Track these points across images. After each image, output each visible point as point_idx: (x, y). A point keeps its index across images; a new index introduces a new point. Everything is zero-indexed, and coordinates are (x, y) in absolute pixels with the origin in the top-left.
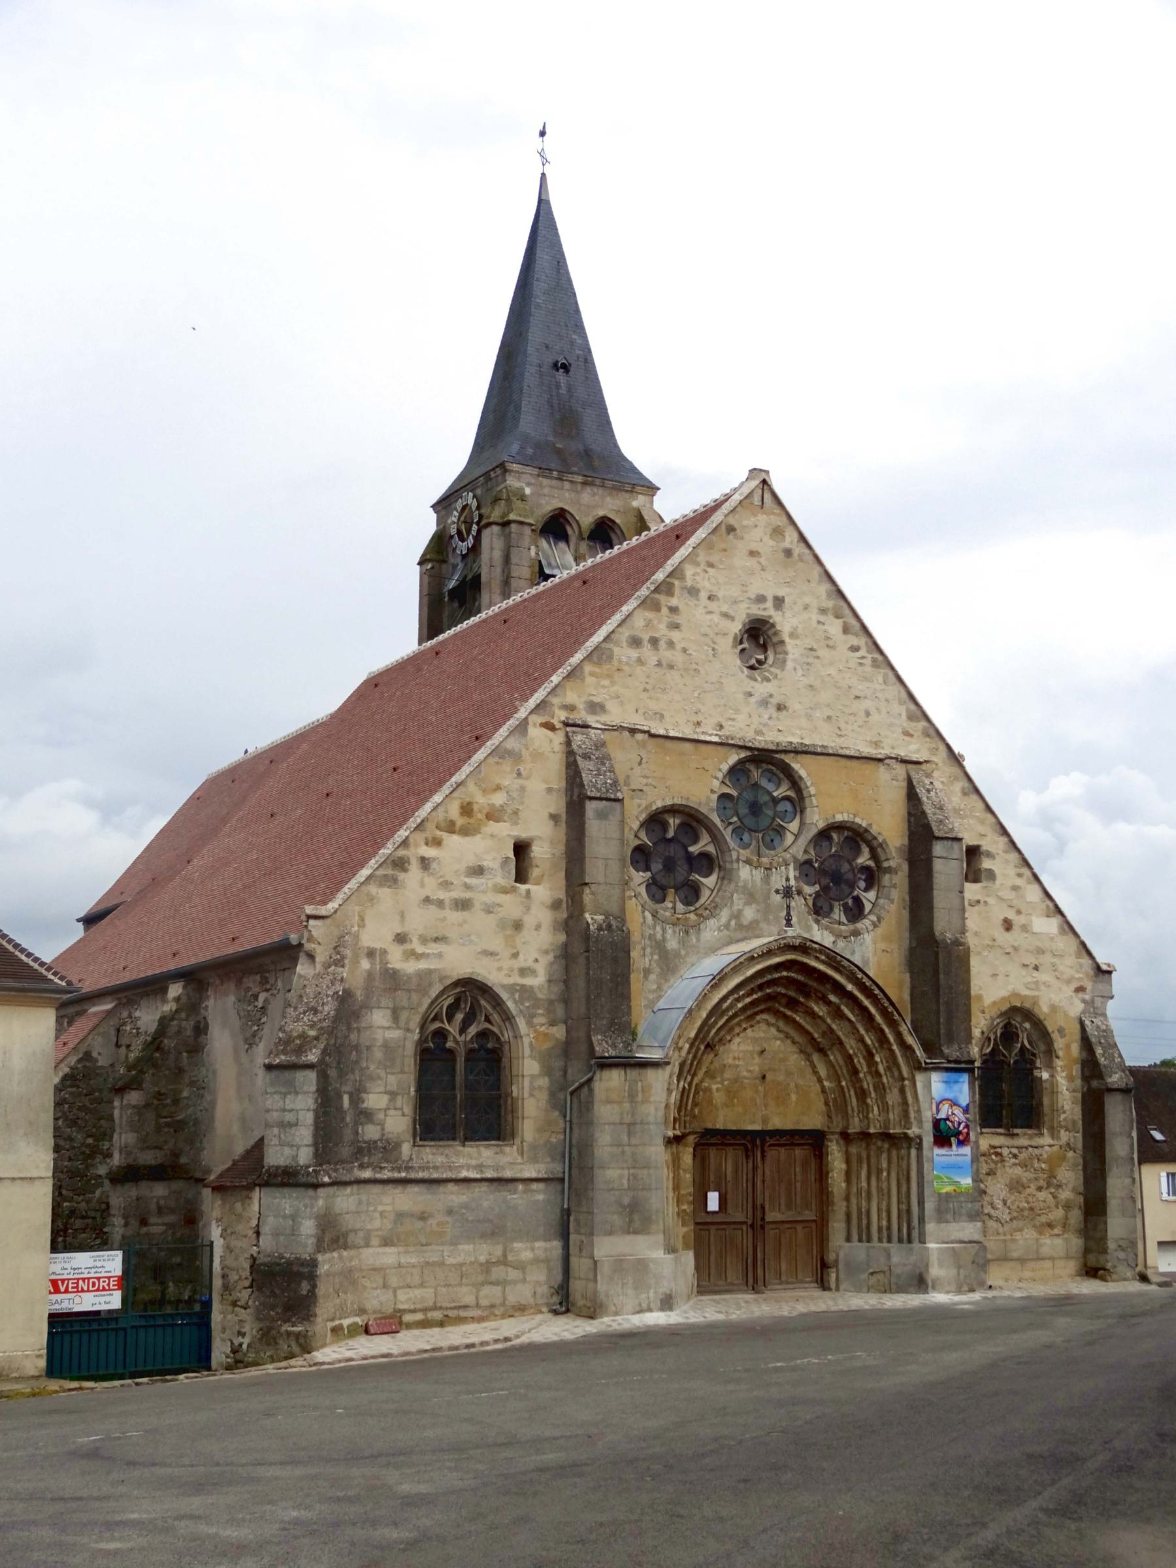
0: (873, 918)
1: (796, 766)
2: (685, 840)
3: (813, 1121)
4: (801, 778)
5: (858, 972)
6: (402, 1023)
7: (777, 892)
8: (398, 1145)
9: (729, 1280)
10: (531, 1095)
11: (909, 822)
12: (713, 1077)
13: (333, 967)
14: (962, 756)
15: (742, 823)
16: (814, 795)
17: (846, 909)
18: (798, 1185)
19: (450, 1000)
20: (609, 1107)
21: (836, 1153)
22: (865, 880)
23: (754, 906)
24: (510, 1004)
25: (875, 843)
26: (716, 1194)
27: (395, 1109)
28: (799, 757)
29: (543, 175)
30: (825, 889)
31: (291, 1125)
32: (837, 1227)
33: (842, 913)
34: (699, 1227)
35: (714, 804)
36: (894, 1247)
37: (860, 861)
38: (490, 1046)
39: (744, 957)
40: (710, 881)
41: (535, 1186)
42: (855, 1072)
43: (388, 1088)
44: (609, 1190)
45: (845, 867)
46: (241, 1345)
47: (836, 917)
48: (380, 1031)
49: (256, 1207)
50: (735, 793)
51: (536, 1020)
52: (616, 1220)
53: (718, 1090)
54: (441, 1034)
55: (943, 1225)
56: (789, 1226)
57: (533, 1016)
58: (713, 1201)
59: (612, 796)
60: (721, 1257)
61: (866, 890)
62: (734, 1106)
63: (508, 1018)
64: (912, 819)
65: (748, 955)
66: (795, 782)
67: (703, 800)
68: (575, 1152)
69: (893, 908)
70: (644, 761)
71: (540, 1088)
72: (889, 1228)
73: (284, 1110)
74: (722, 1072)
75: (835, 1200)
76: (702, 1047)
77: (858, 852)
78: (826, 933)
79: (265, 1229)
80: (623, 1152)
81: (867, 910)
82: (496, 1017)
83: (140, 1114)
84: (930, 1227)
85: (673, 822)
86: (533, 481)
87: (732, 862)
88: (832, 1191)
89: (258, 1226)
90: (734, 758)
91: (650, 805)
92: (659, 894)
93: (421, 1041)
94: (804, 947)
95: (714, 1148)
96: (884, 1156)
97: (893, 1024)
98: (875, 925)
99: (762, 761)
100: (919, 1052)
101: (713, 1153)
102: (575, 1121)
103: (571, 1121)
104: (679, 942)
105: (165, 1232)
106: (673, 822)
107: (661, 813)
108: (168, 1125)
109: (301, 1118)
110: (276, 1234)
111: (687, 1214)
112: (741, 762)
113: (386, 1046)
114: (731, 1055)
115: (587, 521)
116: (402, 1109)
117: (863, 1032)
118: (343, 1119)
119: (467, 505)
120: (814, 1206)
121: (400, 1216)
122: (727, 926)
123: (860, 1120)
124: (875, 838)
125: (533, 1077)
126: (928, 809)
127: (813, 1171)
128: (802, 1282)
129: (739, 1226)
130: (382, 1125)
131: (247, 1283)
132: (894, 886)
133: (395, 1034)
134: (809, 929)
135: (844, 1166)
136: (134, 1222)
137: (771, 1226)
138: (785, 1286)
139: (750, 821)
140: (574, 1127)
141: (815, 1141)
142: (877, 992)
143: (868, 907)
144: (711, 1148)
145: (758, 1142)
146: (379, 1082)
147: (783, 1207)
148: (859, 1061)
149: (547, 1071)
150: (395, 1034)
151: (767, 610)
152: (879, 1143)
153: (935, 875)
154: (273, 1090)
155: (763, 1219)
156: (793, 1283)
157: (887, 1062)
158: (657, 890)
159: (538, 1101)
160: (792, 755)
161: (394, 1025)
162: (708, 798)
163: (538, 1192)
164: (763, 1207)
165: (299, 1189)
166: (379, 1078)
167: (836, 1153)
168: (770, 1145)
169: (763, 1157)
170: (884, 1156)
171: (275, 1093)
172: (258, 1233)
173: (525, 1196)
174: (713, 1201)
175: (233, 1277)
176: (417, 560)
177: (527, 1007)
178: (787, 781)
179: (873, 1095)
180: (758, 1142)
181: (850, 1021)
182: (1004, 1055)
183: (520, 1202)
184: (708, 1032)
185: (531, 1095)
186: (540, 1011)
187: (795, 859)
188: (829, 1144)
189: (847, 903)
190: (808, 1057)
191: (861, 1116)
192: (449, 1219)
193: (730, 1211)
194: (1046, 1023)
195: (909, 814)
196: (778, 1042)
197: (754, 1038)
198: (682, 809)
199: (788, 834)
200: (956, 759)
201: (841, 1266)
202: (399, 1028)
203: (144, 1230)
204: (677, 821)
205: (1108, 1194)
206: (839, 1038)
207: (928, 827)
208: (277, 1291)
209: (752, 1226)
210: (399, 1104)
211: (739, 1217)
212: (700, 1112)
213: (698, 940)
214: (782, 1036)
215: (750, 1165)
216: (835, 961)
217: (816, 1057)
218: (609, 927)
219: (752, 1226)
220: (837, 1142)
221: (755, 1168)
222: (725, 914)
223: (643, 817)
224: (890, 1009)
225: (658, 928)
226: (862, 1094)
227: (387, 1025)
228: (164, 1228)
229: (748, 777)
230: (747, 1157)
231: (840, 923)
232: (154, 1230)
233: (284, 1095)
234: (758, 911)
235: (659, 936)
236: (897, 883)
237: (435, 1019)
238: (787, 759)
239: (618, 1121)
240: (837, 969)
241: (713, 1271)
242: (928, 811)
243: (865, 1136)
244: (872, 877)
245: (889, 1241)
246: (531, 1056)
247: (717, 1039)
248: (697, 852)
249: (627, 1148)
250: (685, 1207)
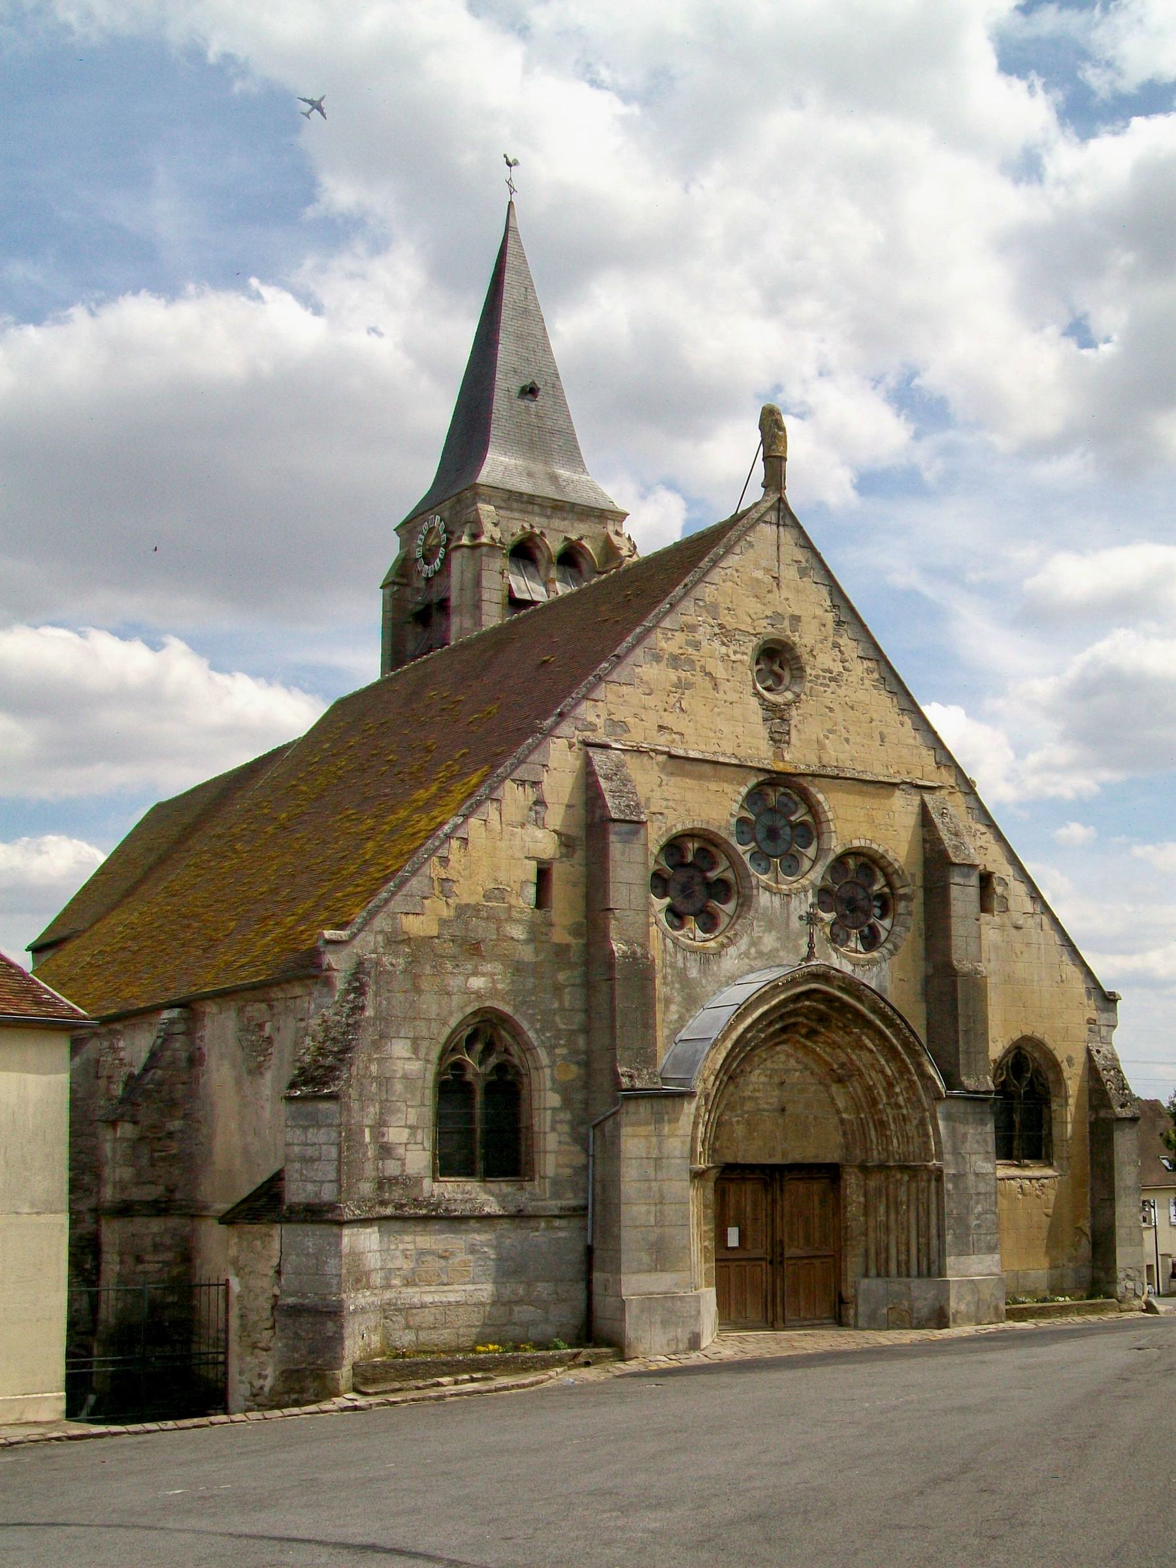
0: (889, 946)
1: (813, 790)
2: (704, 866)
3: (832, 1156)
4: (819, 803)
5: (880, 1001)
6: (422, 1054)
7: (801, 918)
8: (418, 1181)
10: (553, 1129)
11: (924, 848)
12: (733, 1109)
13: (352, 996)
14: (973, 782)
15: (760, 847)
16: (832, 820)
17: (863, 938)
19: (469, 1031)
20: (636, 1140)
22: (880, 908)
23: (773, 933)
24: (531, 1034)
25: (890, 870)
27: (416, 1143)
28: (817, 780)
29: (511, 203)
30: (841, 916)
31: (312, 1160)
32: (853, 1264)
33: (859, 941)
34: (719, 1264)
35: (733, 828)
36: (915, 1282)
37: (876, 887)
38: (509, 1077)
39: (769, 986)
40: (729, 907)
41: (557, 1223)
42: (874, 1102)
43: (408, 1123)
44: (636, 1227)
45: (861, 895)
46: (262, 1388)
47: (852, 945)
48: (399, 1063)
49: (277, 1246)
50: (753, 817)
51: (558, 1051)
52: (645, 1258)
53: (738, 1122)
54: (459, 1066)
55: (963, 1258)
56: (805, 1261)
57: (553, 1047)
58: (733, 1239)
59: (635, 819)
61: (881, 917)
62: (754, 1139)
63: (528, 1048)
64: (928, 846)
65: (772, 984)
66: (813, 808)
67: (723, 824)
68: (598, 1190)
69: (909, 936)
70: (663, 783)
71: (561, 1122)
72: (908, 1262)
73: (307, 1145)
74: (742, 1105)
76: (725, 1078)
77: (873, 881)
78: (844, 961)
79: (287, 1268)
80: (650, 1188)
81: (883, 938)
82: (514, 1049)
83: (133, 1148)
84: (950, 1260)
85: (692, 846)
86: (503, 505)
87: (752, 888)
89: (279, 1265)
90: (753, 781)
91: (670, 828)
92: (676, 922)
93: (439, 1074)
94: (823, 976)
96: (904, 1188)
97: (914, 1054)
98: (891, 953)
99: (778, 785)
100: (941, 1085)
101: (732, 1188)
102: (598, 1155)
103: (593, 1156)
104: (700, 970)
105: (160, 1270)
106: (692, 846)
107: (681, 836)
108: (163, 1159)
109: (324, 1153)
110: (298, 1273)
112: (759, 784)
113: (405, 1077)
114: (751, 1088)
115: (554, 545)
116: (422, 1143)
117: (883, 1062)
118: (365, 1154)
119: (434, 527)
121: (422, 1253)
122: (746, 954)
123: (879, 1153)
124: (891, 864)
125: (554, 1109)
126: (945, 836)
130: (402, 1161)
131: (269, 1324)
132: (910, 914)
133: (415, 1066)
134: (829, 957)
135: (862, 1199)
136: (130, 1260)
139: (768, 847)
140: (598, 1161)
141: (831, 1173)
142: (898, 1022)
143: (883, 935)
145: (777, 1176)
146: (399, 1115)
148: (878, 1093)
149: (567, 1103)
150: (415, 1066)
151: (785, 631)
152: (898, 1176)
153: (953, 902)
154: (294, 1124)
155: (782, 1255)
157: (907, 1093)
158: (676, 915)
159: (560, 1134)
160: (810, 778)
161: (414, 1056)
162: (728, 821)
163: (560, 1229)
164: (781, 1242)
165: (323, 1226)
166: (399, 1111)
169: (782, 1191)
170: (904, 1188)
171: (296, 1126)
172: (279, 1272)
173: (547, 1234)
174: (733, 1239)
175: (253, 1317)
176: (380, 583)
177: (549, 1038)
178: (804, 806)
179: (892, 1127)
180: (777, 1176)
181: (871, 1051)
182: (1015, 1086)
183: (541, 1239)
184: (730, 1065)
185: (553, 1129)
186: (562, 1042)
187: (813, 885)
189: (863, 931)
190: (827, 1087)
191: (880, 1148)
192: (470, 1257)
193: (749, 1246)
194: (1055, 1052)
195: (925, 841)
196: (797, 1074)
197: (775, 1069)
198: (702, 832)
199: (805, 859)
200: (968, 787)
201: (860, 1301)
202: (418, 1059)
203: (140, 1267)
204: (696, 845)
205: (1117, 1224)
206: (859, 1070)
207: (943, 854)
208: (303, 1334)
210: (419, 1138)
211: (759, 1252)
212: (721, 1147)
213: (719, 967)
214: (800, 1067)
215: (769, 1197)
216: (858, 990)
217: (834, 1088)
218: (634, 953)
219: (771, 1262)
220: (855, 1175)
221: (774, 1201)
222: (743, 943)
223: (663, 841)
224: (912, 1039)
225: (679, 956)
226: (881, 1125)
227: (408, 1055)
228: (161, 1265)
229: (765, 800)
230: (766, 1190)
231: (856, 951)
232: (149, 1267)
233: (305, 1128)
234: (778, 938)
235: (680, 964)
236: (912, 910)
237: (453, 1050)
238: (805, 782)
239: (644, 1155)
240: (859, 999)
242: (944, 837)
243: (882, 1167)
244: (886, 905)
245: (908, 1276)
246: (551, 1089)
247: (738, 1071)
248: (715, 878)
249: (653, 1184)
250: (706, 1244)
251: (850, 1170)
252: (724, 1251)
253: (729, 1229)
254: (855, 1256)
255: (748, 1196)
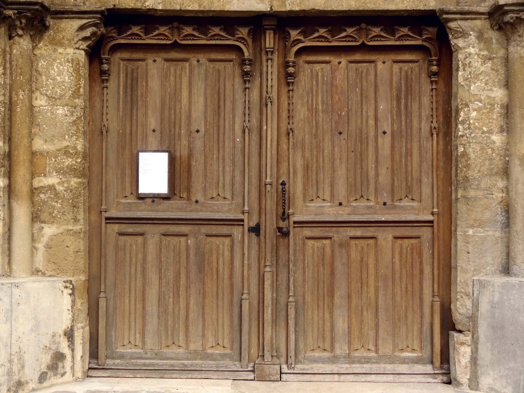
9: (192, 347)
18: (385, 143)
21: (477, 63)
26: (164, 157)
56: (358, 232)
60: (177, 295)
75: (472, 173)
88: (465, 154)
95: (160, 57)
111: (57, 194)
120: (426, 190)
127: (426, 112)
128: (392, 360)
129: (225, 230)
137: (308, 232)
138: (344, 367)
144: (150, 57)
147: (341, 192)
155: (285, 216)
156: (368, 360)
167: (477, 63)
168: (299, 53)
188: (460, 43)
209: (256, 230)
215: (255, 94)
219: (256, 230)
220: (480, 36)
230: (246, 76)
241: (153, 323)
251: (464, 25)
252: (131, 200)
253: (143, 156)
254: (480, 224)
255: (199, 87)
